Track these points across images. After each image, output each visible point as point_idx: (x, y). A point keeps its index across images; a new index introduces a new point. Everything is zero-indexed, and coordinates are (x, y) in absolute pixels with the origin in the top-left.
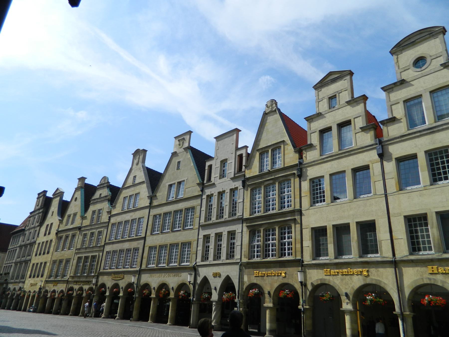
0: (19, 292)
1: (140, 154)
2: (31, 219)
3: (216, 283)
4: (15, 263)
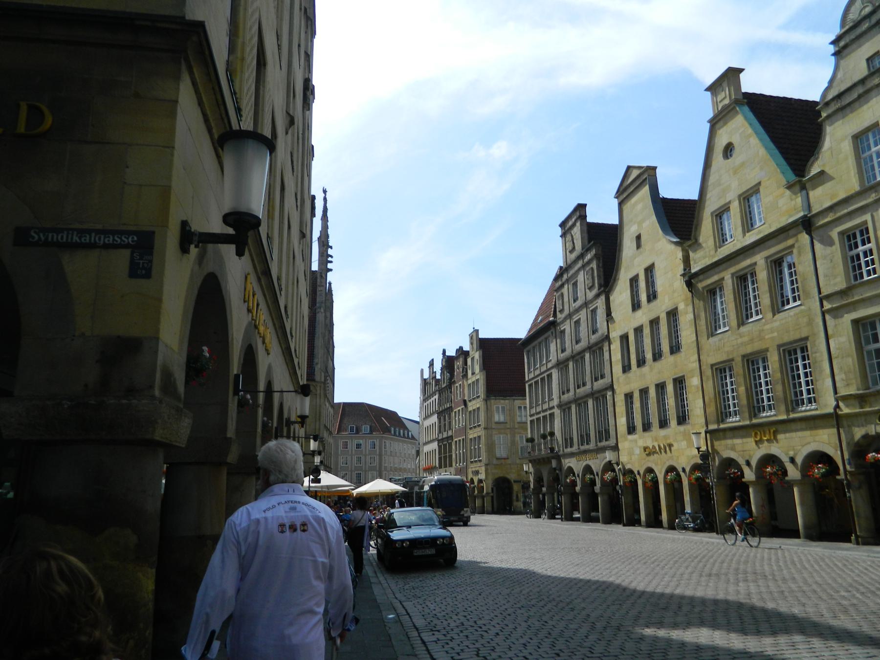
0: (608, 476)
2: (565, 290)
4: (560, 406)
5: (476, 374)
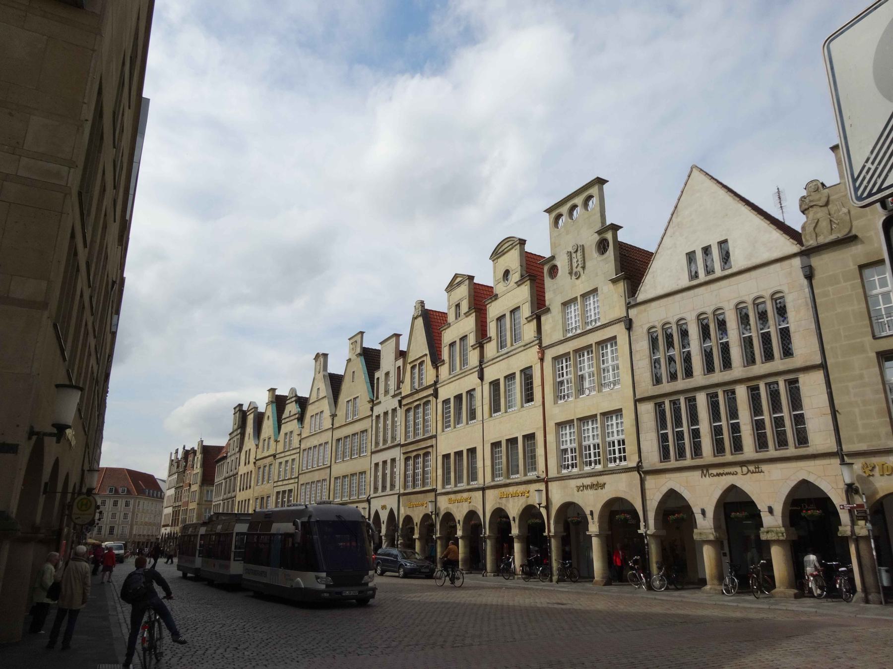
1: (322, 358)
3: (384, 516)
5: (198, 469)
